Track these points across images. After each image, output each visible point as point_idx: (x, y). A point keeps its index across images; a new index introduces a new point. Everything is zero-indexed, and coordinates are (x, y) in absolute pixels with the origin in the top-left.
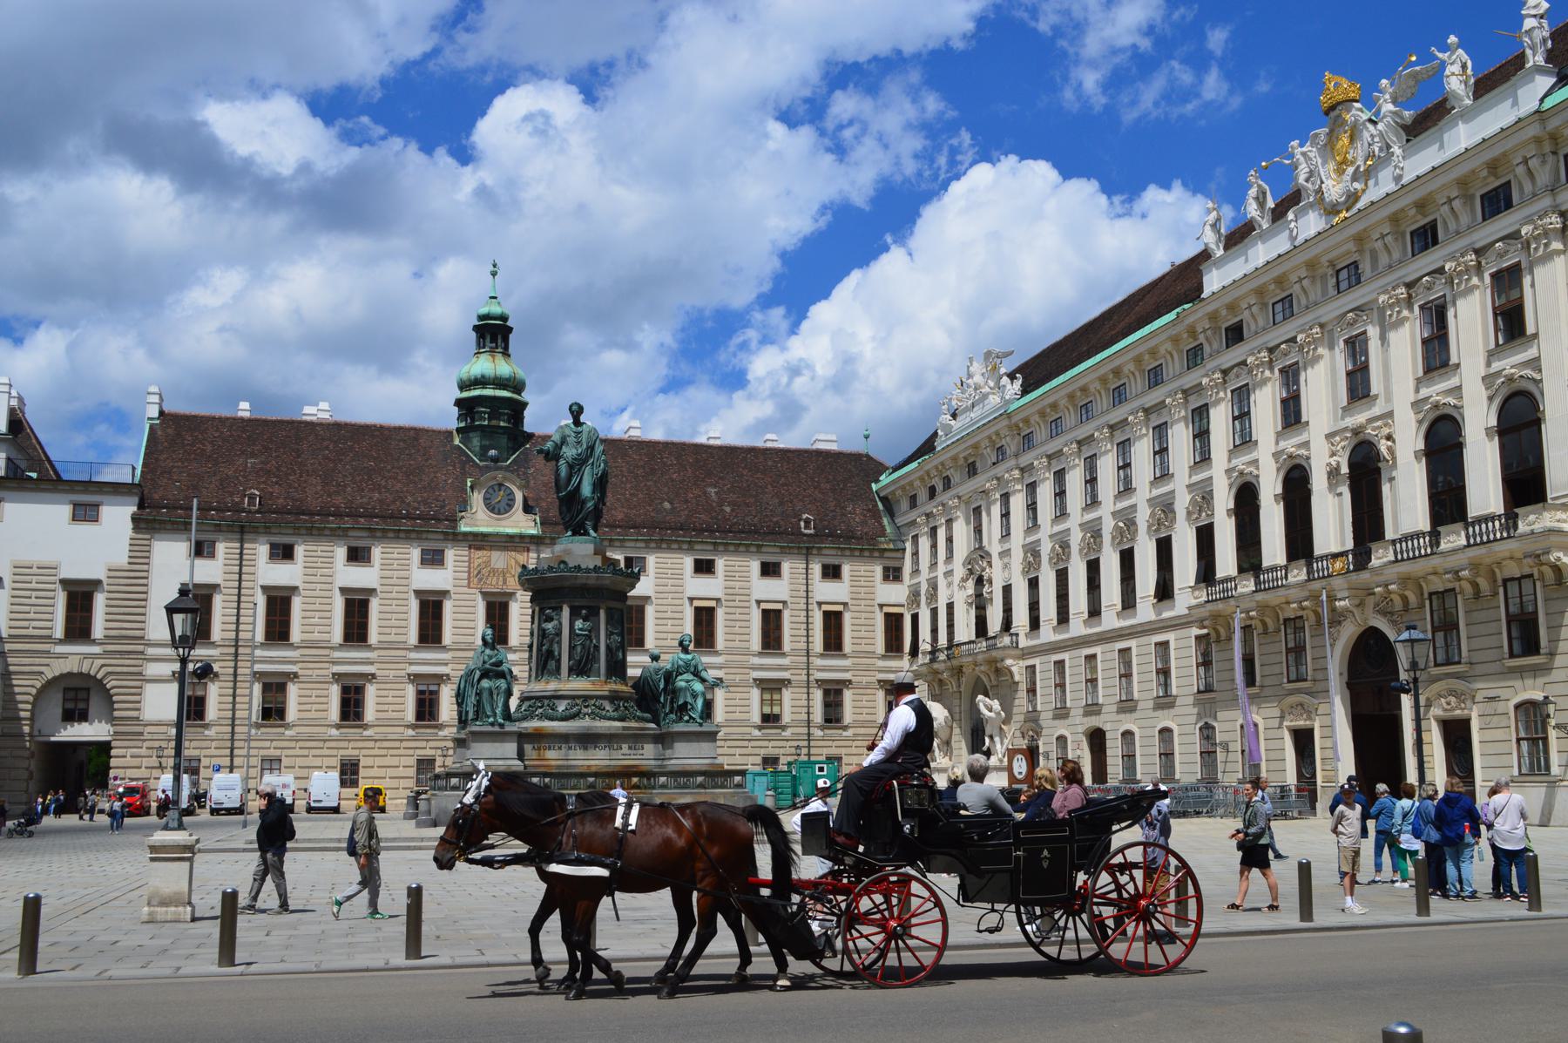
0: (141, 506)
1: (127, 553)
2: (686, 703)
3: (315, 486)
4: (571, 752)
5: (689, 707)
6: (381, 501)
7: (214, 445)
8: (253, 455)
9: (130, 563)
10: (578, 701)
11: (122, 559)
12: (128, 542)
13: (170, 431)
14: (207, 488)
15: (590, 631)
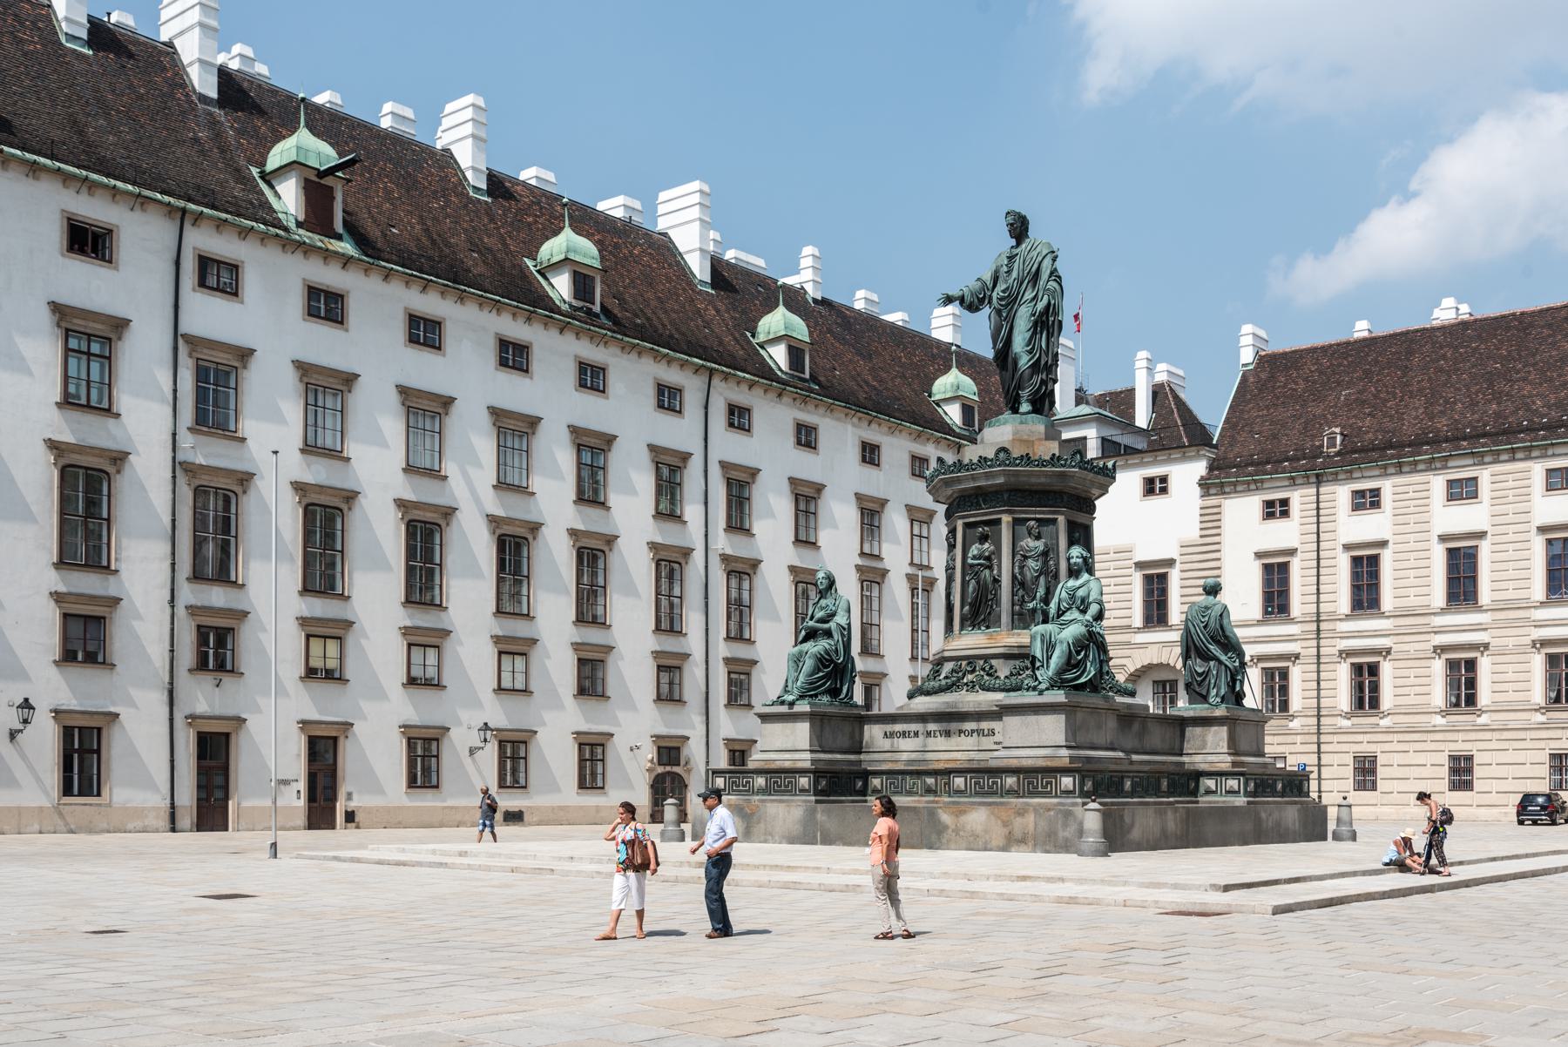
0: (1211, 468)
1: (1198, 526)
2: (1034, 657)
3: (1416, 409)
4: (931, 740)
5: (1038, 664)
6: (1498, 415)
7: (1308, 381)
8: (1349, 385)
9: (1201, 536)
10: (964, 663)
11: (1192, 532)
12: (1198, 512)
13: (1263, 376)
14: (1286, 435)
15: (988, 558)
